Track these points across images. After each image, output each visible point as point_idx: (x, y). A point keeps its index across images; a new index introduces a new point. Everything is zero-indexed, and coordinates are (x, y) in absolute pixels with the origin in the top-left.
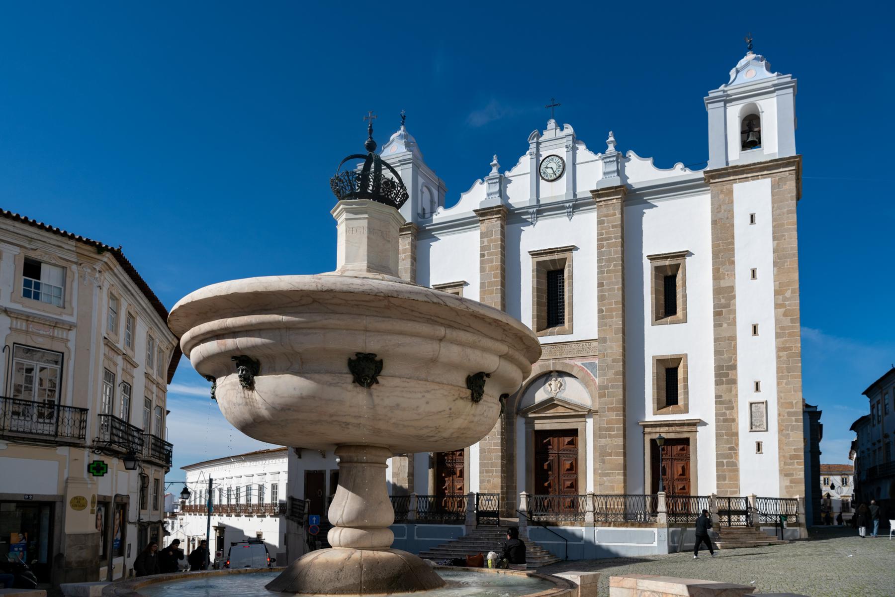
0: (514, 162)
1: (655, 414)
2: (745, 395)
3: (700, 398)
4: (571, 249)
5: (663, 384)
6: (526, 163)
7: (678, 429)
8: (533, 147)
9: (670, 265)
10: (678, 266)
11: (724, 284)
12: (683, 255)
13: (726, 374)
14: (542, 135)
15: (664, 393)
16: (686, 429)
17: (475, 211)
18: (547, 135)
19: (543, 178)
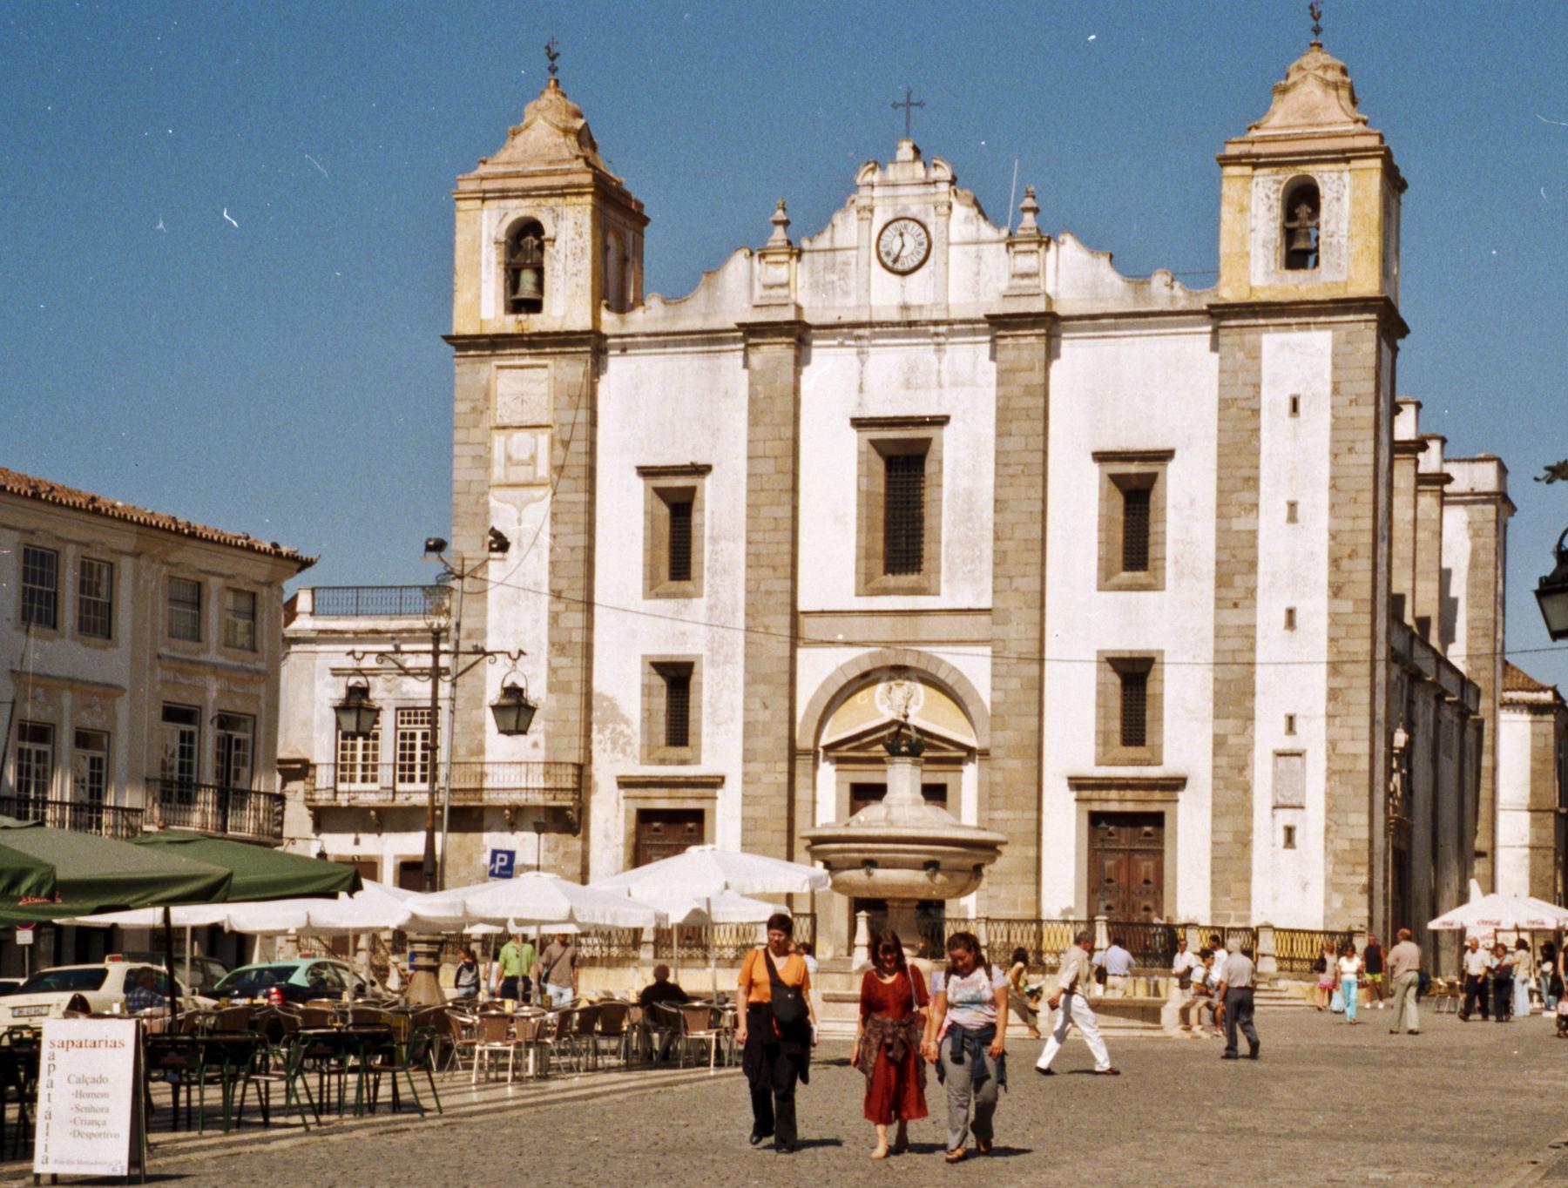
0: (822, 223)
1: (1098, 763)
2: (1268, 735)
3: (1184, 736)
4: (941, 421)
5: (1116, 703)
6: (847, 229)
7: (1142, 794)
8: (862, 198)
9: (1138, 475)
10: (1152, 478)
11: (1239, 524)
12: (1165, 456)
13: (1234, 695)
14: (883, 168)
15: (1116, 725)
16: (1157, 795)
17: (741, 326)
18: (893, 173)
19: (884, 265)
